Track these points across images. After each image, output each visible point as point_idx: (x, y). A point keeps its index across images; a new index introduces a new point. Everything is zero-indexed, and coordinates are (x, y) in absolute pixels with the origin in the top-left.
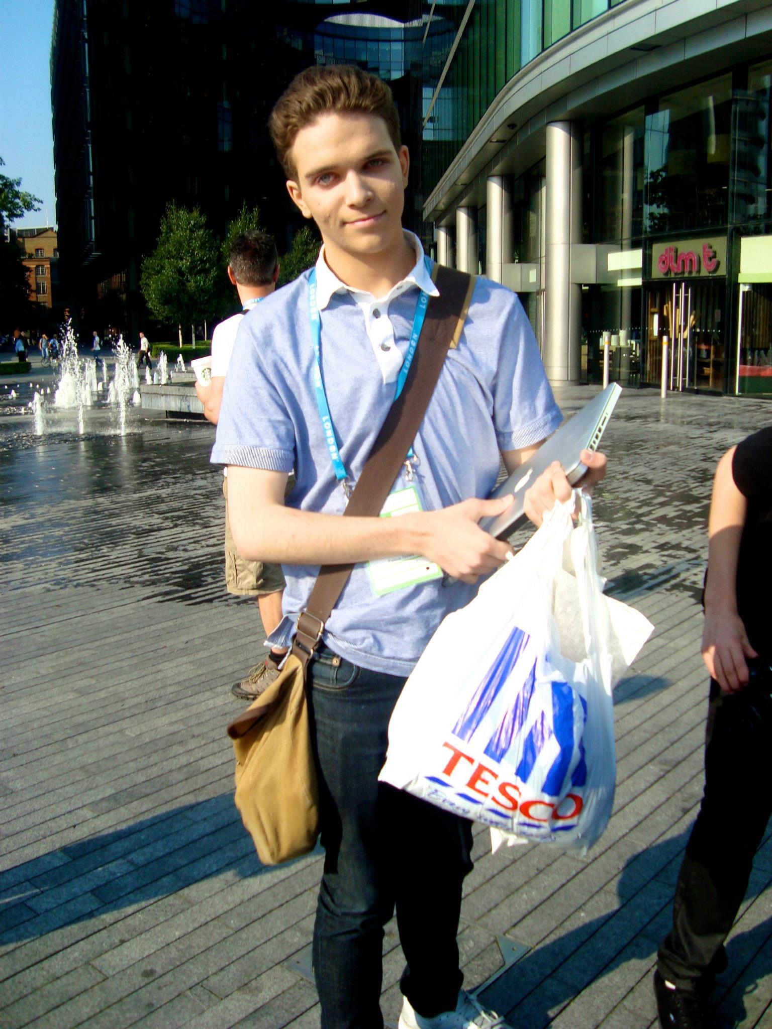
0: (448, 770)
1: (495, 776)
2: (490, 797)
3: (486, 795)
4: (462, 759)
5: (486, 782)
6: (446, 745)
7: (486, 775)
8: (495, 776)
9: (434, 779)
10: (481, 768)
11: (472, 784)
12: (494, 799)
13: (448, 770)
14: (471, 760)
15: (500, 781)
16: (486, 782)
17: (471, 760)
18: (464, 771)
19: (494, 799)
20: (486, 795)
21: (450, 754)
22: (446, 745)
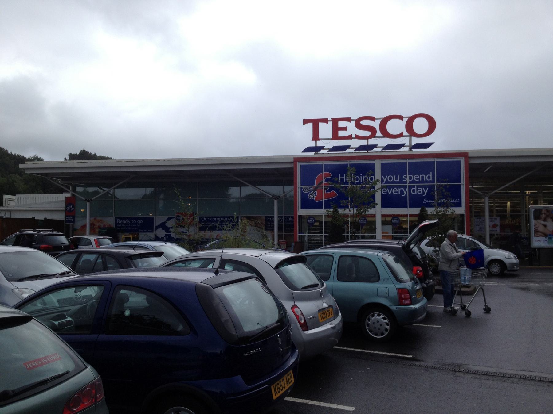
0: (316, 137)
1: (349, 120)
2: (353, 136)
3: (349, 137)
4: (321, 125)
5: (345, 129)
6: (306, 122)
7: (341, 124)
8: (349, 120)
10: (335, 121)
11: (335, 137)
12: (357, 137)
14: (326, 121)
16: (345, 129)
17: (326, 121)
18: (326, 130)
19: (357, 137)
20: (349, 137)
21: (310, 125)
22: (306, 122)
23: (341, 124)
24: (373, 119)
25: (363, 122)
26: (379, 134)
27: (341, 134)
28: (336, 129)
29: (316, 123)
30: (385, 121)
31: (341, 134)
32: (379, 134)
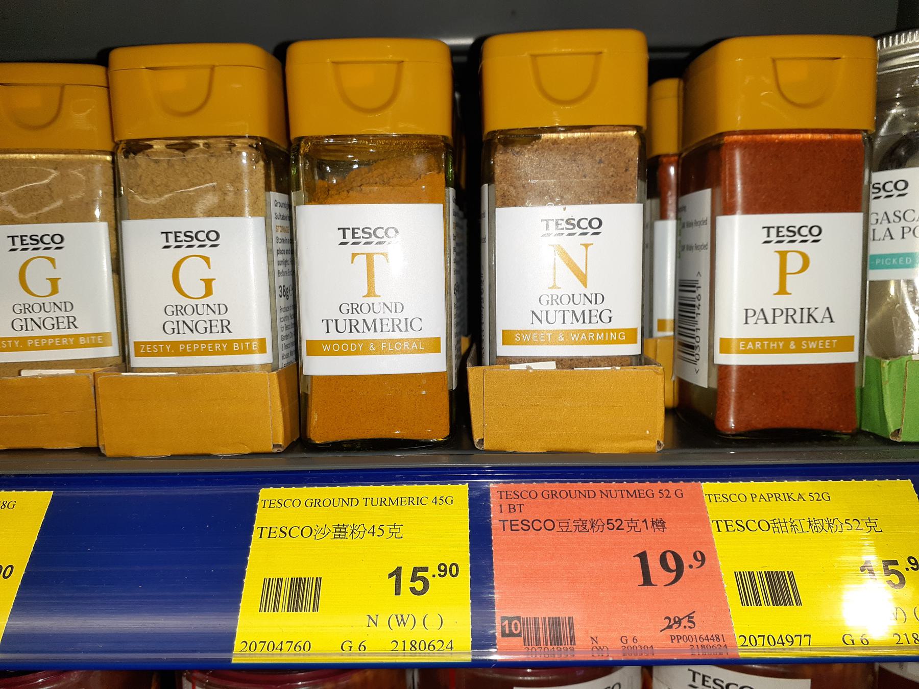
1: (358, 228)
4: (346, 230)
5: (357, 233)
6: (339, 229)
7: (356, 231)
8: (358, 228)
9: (342, 244)
10: (353, 229)
11: (354, 237)
12: (363, 237)
13: (344, 237)
14: (349, 229)
15: (361, 229)
16: (357, 233)
17: (349, 229)
18: (349, 233)
19: (363, 237)
21: (342, 230)
22: (339, 229)
23: (356, 231)
24: (370, 228)
25: (366, 230)
26: (373, 236)
27: (356, 235)
28: (354, 233)
29: (344, 229)
30: (375, 232)
31: (356, 235)
32: (373, 236)
